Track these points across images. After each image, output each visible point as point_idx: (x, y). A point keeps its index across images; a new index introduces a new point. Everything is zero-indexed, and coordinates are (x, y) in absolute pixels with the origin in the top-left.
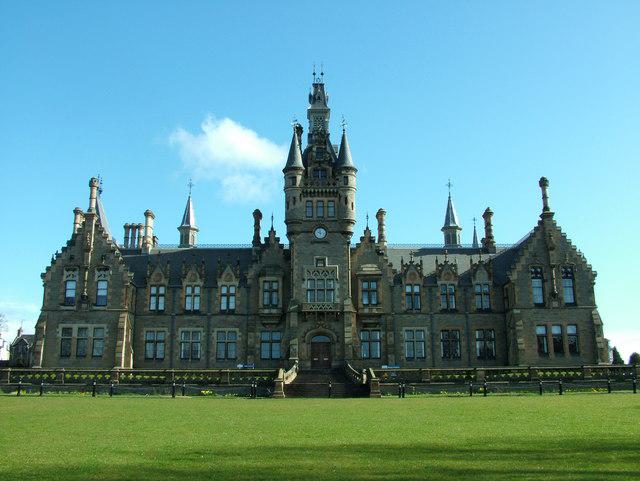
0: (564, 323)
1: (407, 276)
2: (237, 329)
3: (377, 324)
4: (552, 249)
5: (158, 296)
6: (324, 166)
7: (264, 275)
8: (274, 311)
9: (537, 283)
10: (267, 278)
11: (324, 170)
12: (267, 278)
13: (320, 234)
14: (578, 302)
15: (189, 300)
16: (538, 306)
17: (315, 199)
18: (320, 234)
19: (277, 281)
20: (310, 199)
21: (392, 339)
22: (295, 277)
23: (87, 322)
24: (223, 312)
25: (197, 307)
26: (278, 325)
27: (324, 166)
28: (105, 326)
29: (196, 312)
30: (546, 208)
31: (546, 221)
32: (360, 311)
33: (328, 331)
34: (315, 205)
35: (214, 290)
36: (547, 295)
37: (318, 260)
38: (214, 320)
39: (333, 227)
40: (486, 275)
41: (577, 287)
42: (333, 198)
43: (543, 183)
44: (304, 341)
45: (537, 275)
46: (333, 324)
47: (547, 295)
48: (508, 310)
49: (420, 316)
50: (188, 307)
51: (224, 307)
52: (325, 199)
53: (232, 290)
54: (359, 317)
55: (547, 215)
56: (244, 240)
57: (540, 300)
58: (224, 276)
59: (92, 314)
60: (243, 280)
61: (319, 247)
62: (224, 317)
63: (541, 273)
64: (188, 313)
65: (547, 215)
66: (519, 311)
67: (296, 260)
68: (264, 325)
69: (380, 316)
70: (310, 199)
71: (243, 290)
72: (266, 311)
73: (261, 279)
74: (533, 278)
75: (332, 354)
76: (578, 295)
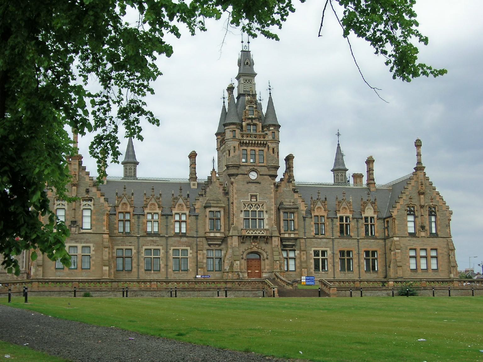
0: (429, 249)
1: (315, 210)
2: (189, 248)
3: (293, 245)
4: (423, 194)
5: (180, 222)
6: (254, 122)
7: (210, 207)
8: (218, 235)
9: (411, 218)
10: (212, 209)
11: (255, 125)
12: (212, 209)
13: (253, 176)
14: (439, 233)
15: (149, 224)
16: (411, 235)
17: (249, 148)
18: (253, 176)
19: (219, 212)
20: (245, 148)
21: (305, 257)
22: (235, 209)
23: (77, 242)
24: (176, 235)
25: (156, 229)
26: (220, 245)
27: (254, 122)
28: (91, 245)
29: (156, 235)
30: (419, 163)
31: (419, 172)
32: (282, 236)
33: (260, 251)
34: (249, 153)
35: (170, 217)
36: (418, 228)
37: (252, 196)
38: (171, 241)
39: (264, 171)
40: (373, 211)
41: (438, 222)
42: (263, 148)
43: (418, 144)
44: (242, 258)
45: (411, 212)
46: (263, 245)
47: (418, 228)
48: (388, 237)
49: (325, 240)
50: (149, 229)
51: (177, 230)
52: (257, 149)
53: (184, 218)
54: (282, 240)
55: (419, 168)
56: (181, 173)
57: (411, 230)
58: (177, 207)
59: (82, 236)
60: (192, 210)
61: (253, 187)
62: (178, 239)
63: (414, 212)
64: (150, 235)
65: (419, 168)
66: (398, 239)
67: (235, 196)
68: (209, 245)
69: (296, 239)
70: (245, 148)
71: (193, 218)
72: (212, 235)
73: (208, 210)
74: (408, 214)
75: (262, 267)
76: (439, 228)
